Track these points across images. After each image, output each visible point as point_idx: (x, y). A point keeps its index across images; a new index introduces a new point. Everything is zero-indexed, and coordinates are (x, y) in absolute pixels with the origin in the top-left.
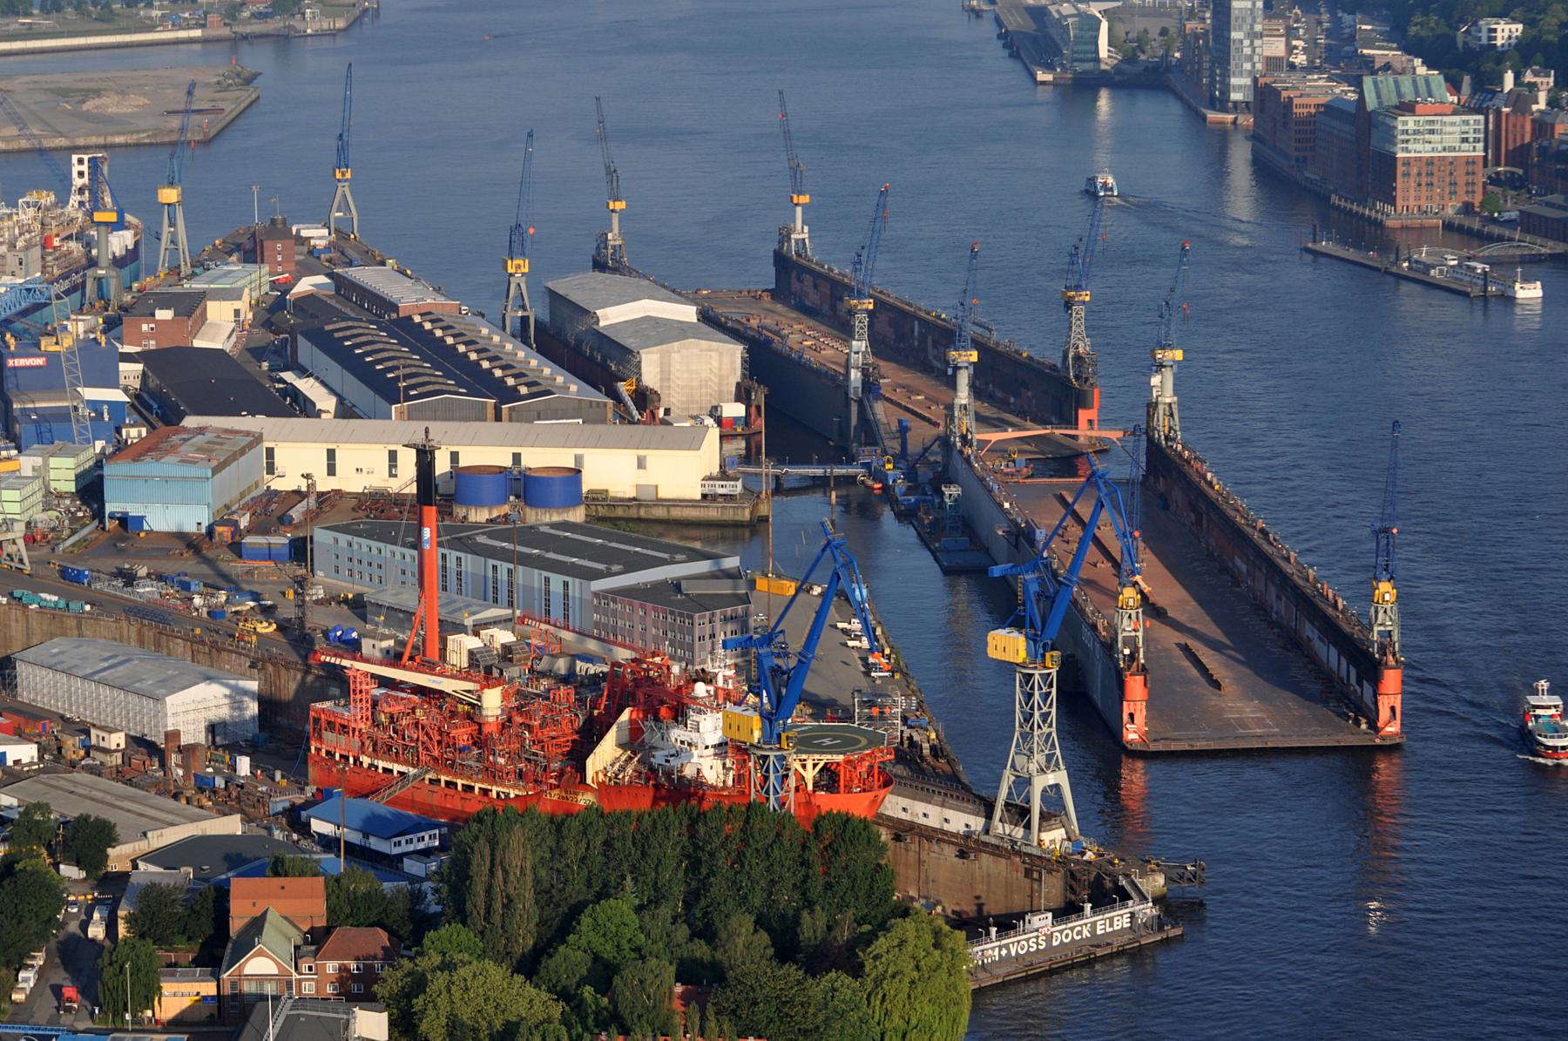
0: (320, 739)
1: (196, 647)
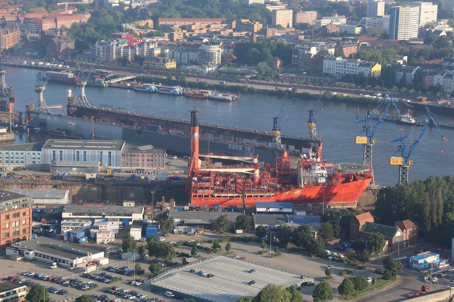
0: (196, 192)
1: (23, 186)
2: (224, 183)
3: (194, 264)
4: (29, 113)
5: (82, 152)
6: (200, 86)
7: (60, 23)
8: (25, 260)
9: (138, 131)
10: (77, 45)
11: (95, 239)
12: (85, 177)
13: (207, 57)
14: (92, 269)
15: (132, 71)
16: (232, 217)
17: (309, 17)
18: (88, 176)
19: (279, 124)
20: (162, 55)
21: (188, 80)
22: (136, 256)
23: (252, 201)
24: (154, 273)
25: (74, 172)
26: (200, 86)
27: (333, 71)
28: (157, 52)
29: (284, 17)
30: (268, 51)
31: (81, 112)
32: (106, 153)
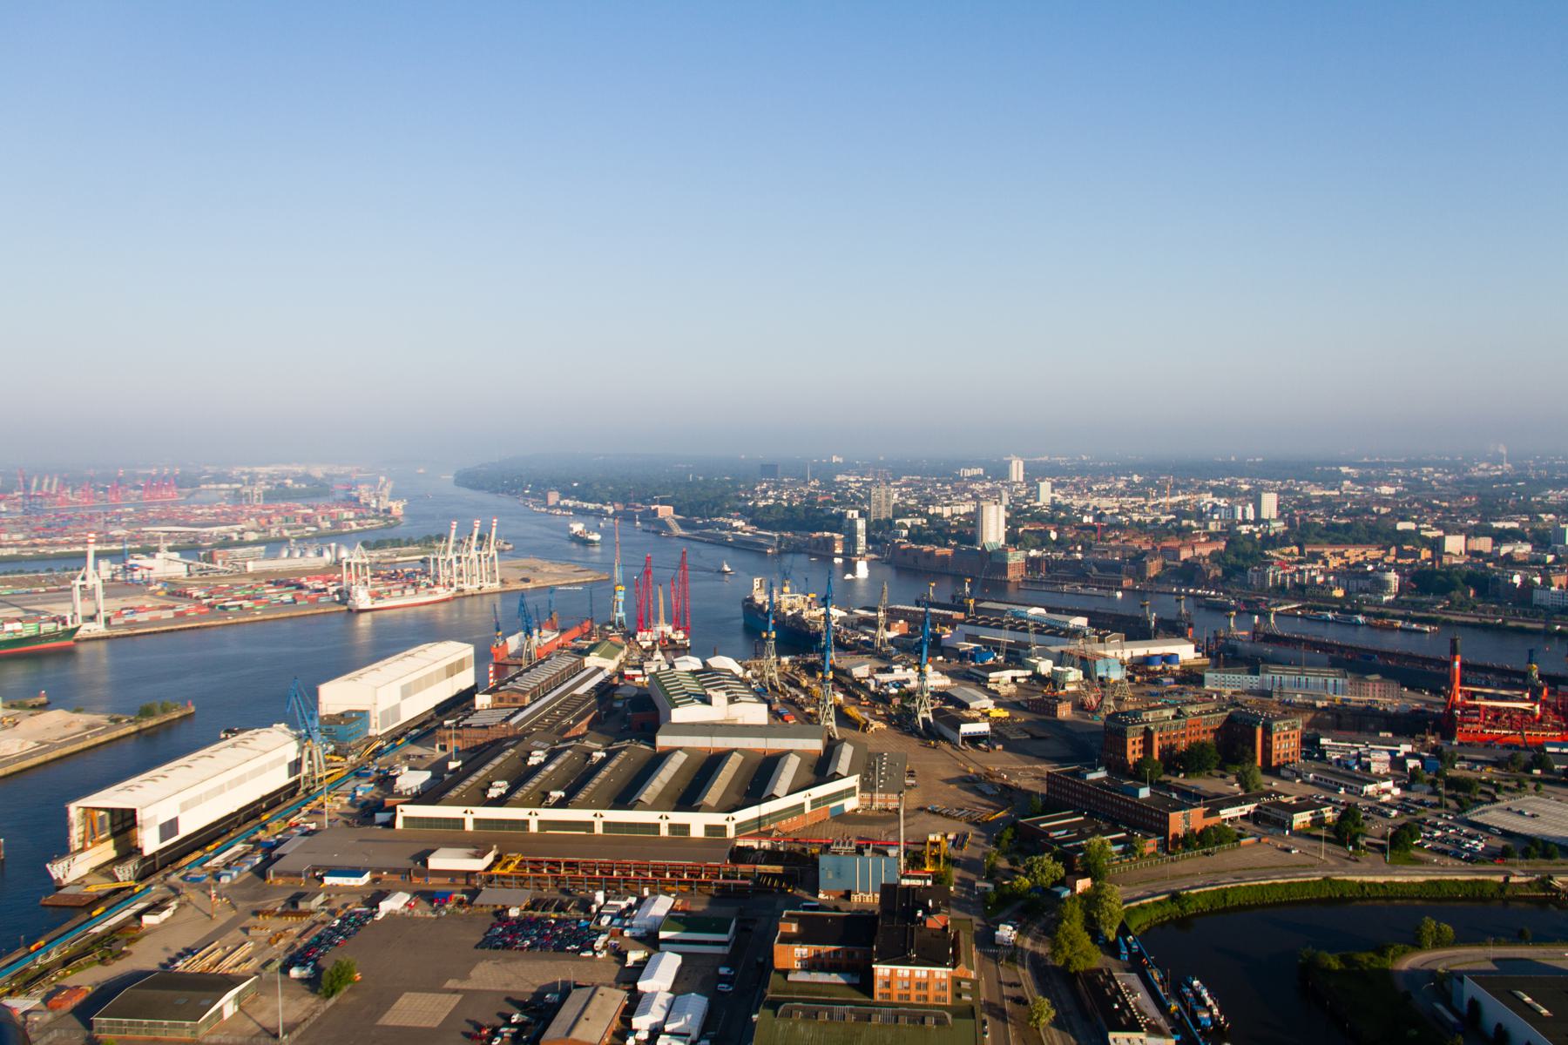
2: (1496, 718)
3: (1505, 801)
4: (1217, 638)
5: (1303, 679)
6: (1381, 616)
7: (1198, 551)
8: (1304, 782)
9: (1356, 662)
10: (1224, 572)
11: (1368, 766)
12: (1314, 705)
13: (1383, 586)
14: (1386, 798)
15: (1296, 600)
16: (1526, 756)
17: (1484, 544)
18: (1319, 704)
19: (1535, 656)
20: (1326, 582)
21: (1366, 609)
22: (1428, 788)
23: (1540, 740)
24: (1463, 807)
25: (1299, 698)
26: (1381, 616)
27: (1547, 602)
28: (1320, 579)
29: (1455, 544)
30: (1458, 579)
31: (1270, 638)
32: (1331, 681)
